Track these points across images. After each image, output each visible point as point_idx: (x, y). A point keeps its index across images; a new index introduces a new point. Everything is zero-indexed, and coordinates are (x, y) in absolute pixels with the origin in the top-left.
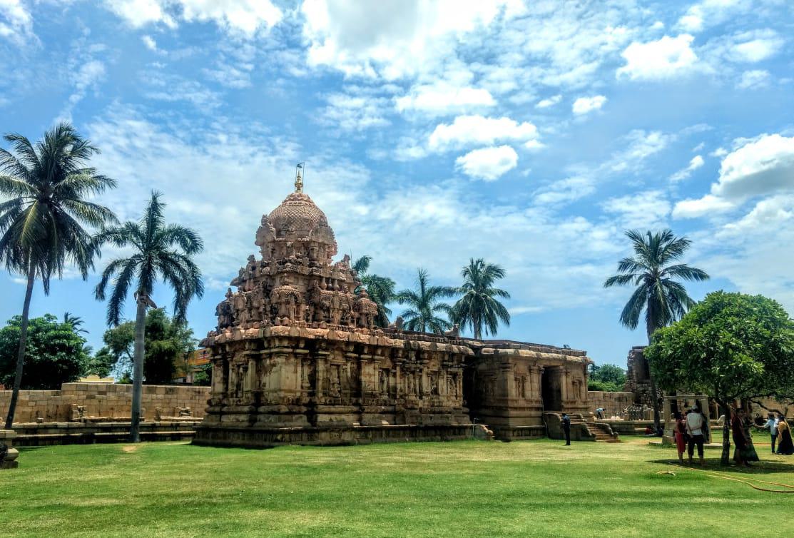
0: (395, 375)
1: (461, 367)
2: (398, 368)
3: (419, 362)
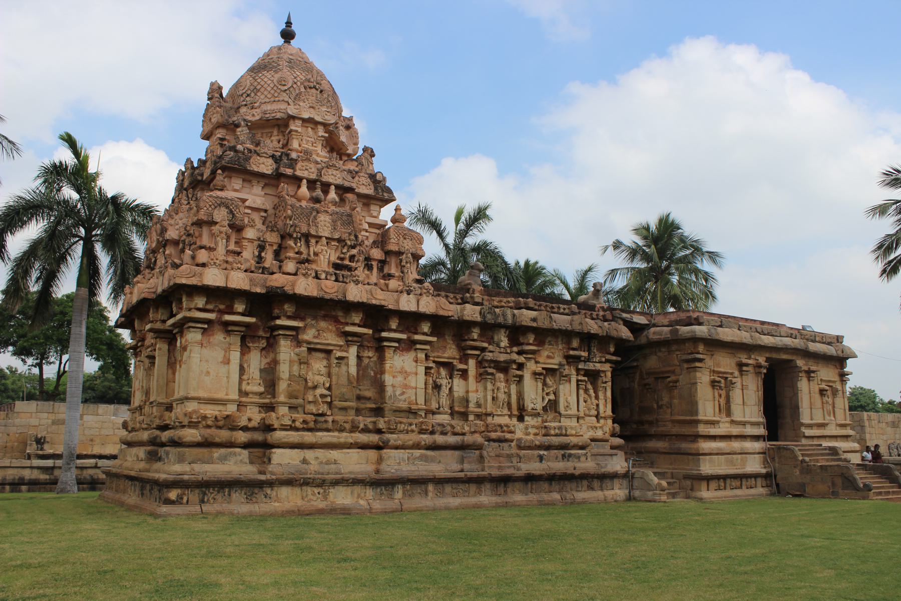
0: (464, 374)
1: (607, 361)
2: (472, 363)
3: (515, 349)
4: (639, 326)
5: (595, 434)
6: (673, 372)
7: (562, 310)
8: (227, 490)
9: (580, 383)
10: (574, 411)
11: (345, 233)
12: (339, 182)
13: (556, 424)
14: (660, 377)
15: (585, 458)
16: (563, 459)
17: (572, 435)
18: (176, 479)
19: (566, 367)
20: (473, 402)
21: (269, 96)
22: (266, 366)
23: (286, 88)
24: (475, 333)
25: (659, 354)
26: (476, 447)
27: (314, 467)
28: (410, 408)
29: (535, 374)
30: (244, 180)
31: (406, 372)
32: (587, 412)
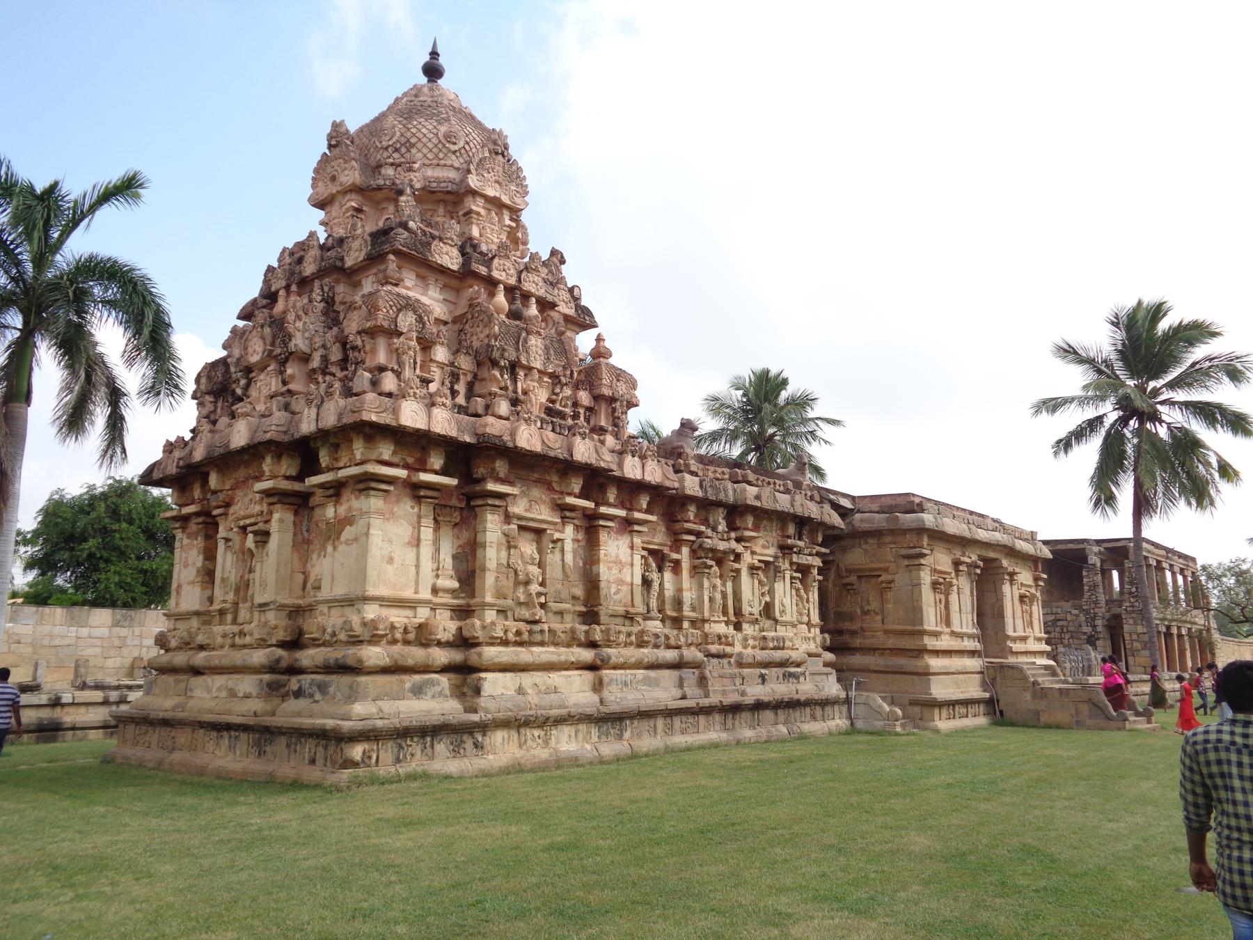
1: (818, 554)
2: (685, 551)
3: (733, 535)
6: (886, 570)
8: (429, 739)
11: (558, 366)
12: (541, 293)
13: (772, 634)
14: (867, 575)
18: (367, 728)
19: (781, 560)
21: (430, 156)
22: (459, 551)
23: (456, 148)
24: (692, 512)
25: (864, 546)
27: (533, 698)
28: (627, 612)
29: (752, 568)
30: (418, 276)
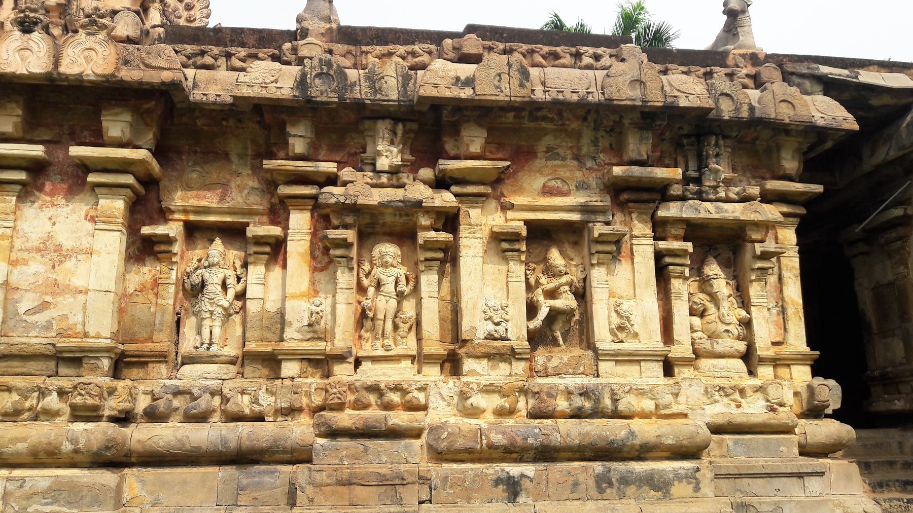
4: (886, 100)
5: (735, 411)
7: (587, 60)
9: (668, 260)
10: (652, 340)
15: (690, 488)
16: (601, 491)
17: (644, 415)
20: (296, 325)
26: (287, 457)
31: (58, 249)
32: (706, 344)
